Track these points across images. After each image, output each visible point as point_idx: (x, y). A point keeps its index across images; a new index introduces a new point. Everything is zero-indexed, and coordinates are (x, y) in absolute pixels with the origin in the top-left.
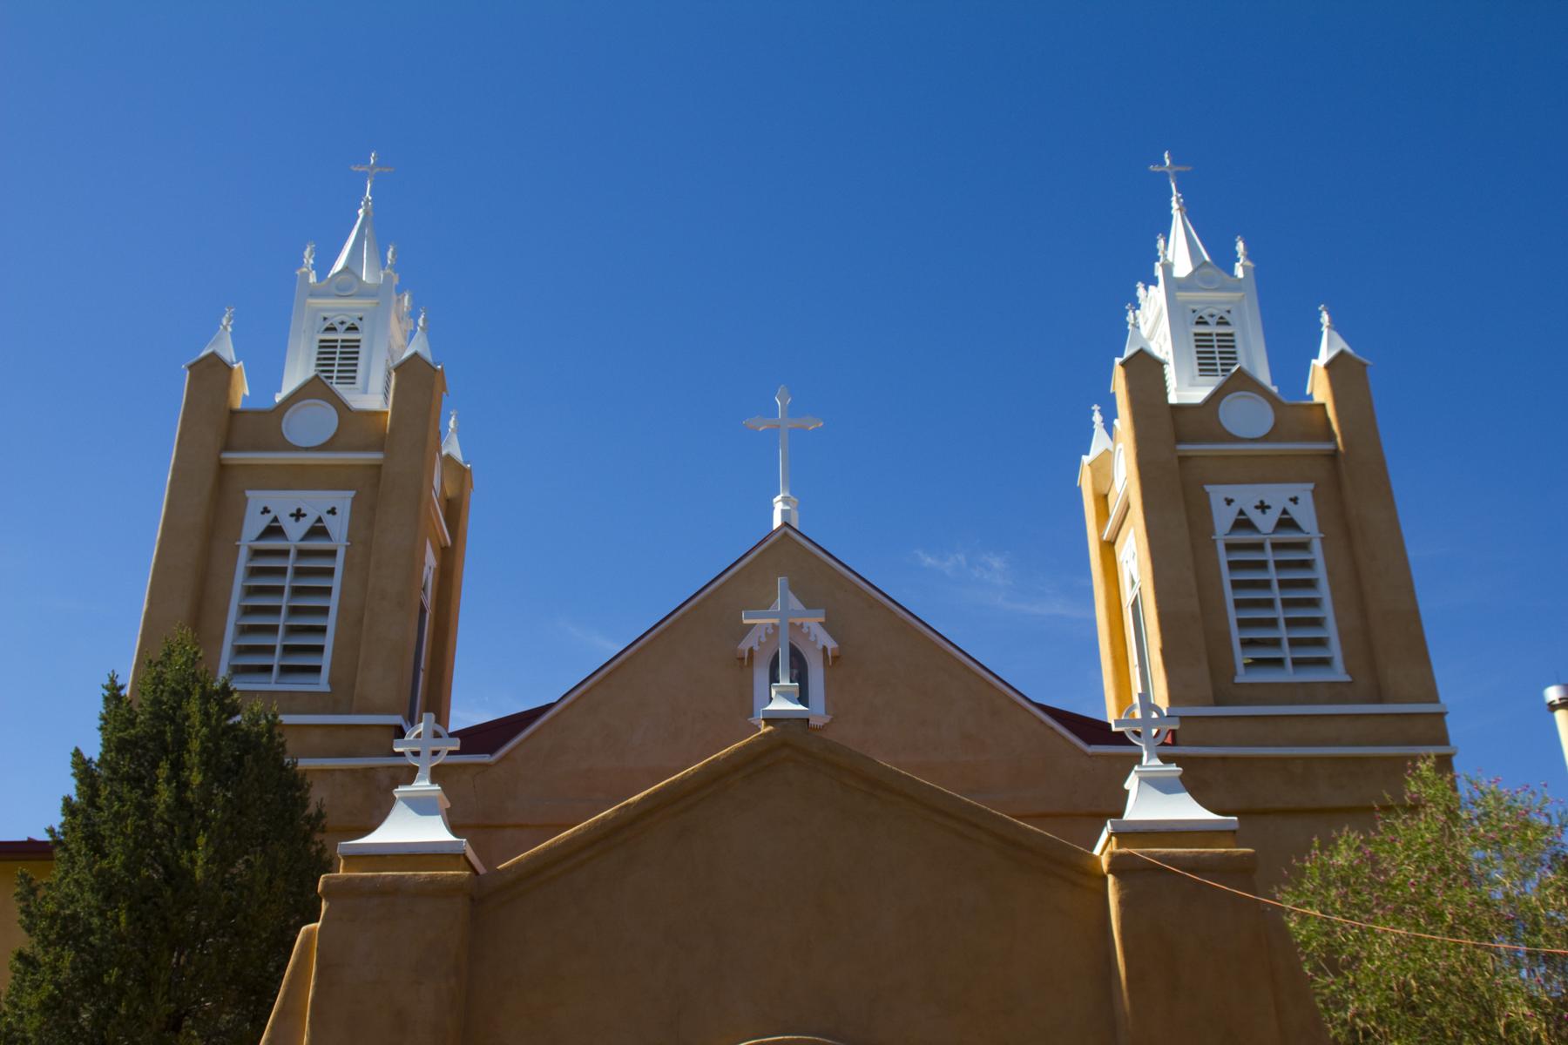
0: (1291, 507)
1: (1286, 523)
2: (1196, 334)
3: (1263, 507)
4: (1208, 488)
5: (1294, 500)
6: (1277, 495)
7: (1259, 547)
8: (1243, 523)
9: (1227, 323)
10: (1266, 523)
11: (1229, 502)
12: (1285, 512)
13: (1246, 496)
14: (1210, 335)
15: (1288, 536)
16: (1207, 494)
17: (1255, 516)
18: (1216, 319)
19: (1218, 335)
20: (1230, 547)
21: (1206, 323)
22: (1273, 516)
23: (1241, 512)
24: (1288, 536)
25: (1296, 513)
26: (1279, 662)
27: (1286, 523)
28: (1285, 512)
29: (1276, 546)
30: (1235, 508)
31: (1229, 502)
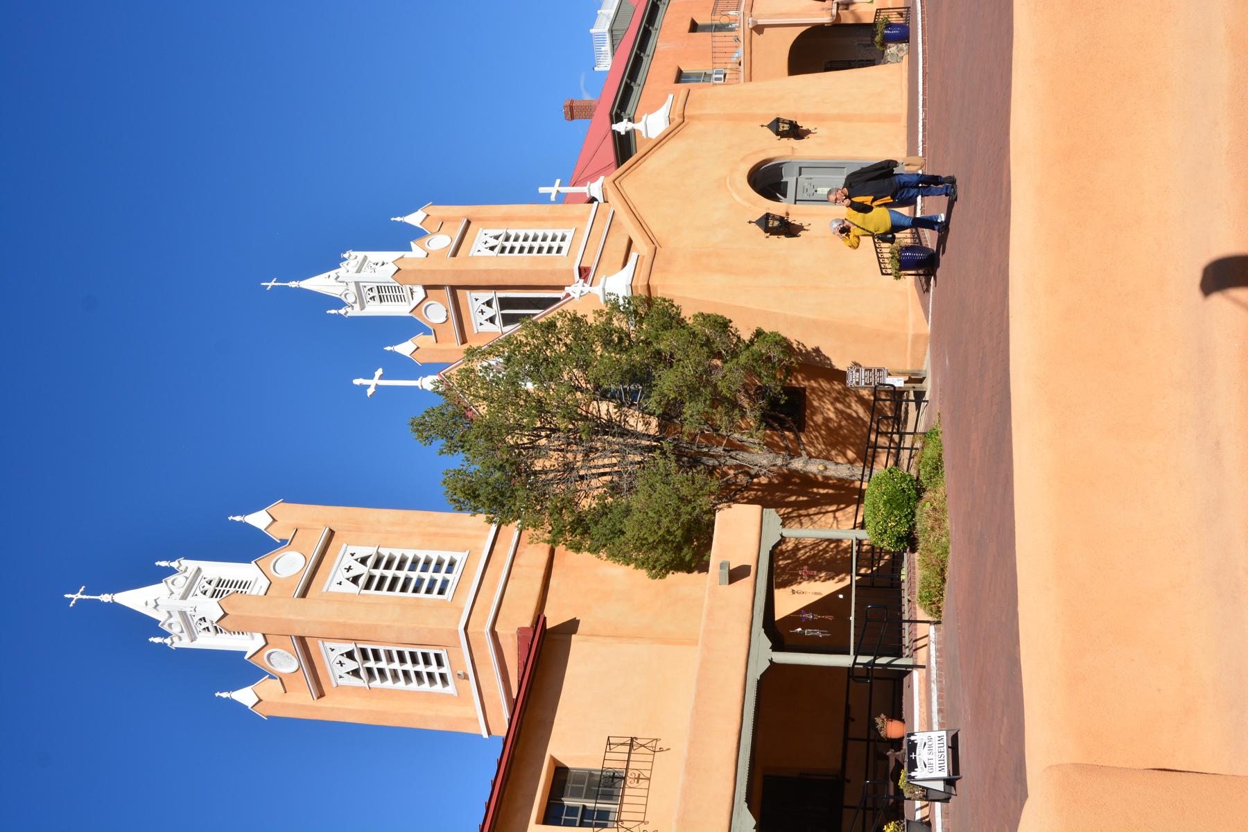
0: (355, 557)
1: (363, 561)
2: (212, 597)
3: (349, 569)
7: (371, 578)
8: (355, 580)
9: (211, 581)
10: (358, 569)
11: (340, 584)
12: (357, 560)
14: (216, 590)
15: (370, 562)
19: (218, 586)
20: (367, 587)
21: (206, 591)
23: (348, 579)
24: (370, 562)
25: (359, 555)
26: (445, 582)
27: (363, 561)
28: (357, 560)
30: (346, 583)
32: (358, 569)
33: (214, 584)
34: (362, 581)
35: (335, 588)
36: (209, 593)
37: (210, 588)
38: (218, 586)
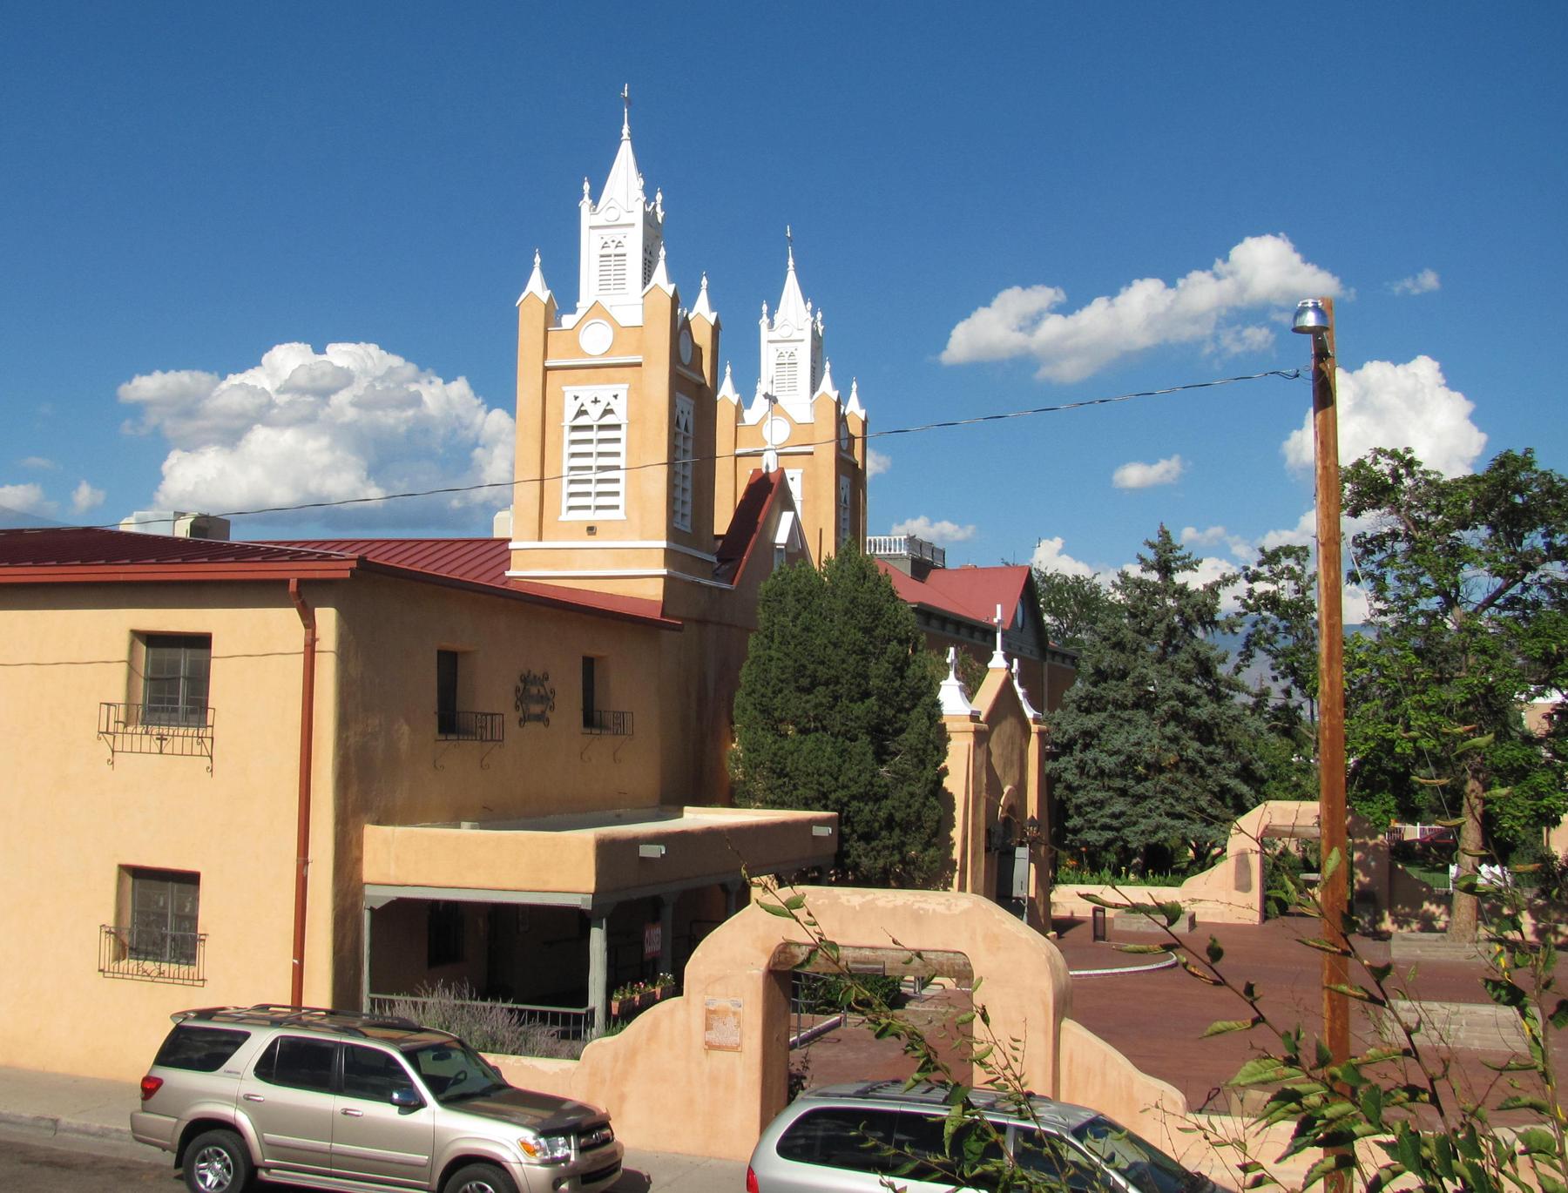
2: (602, 256)
4: (564, 388)
5: (616, 397)
6: (605, 393)
7: (590, 428)
11: (576, 398)
12: (609, 404)
13: (586, 393)
14: (610, 256)
16: (564, 392)
17: (589, 407)
18: (615, 244)
19: (616, 255)
20: (575, 428)
22: (600, 408)
23: (582, 405)
24: (608, 420)
27: (607, 412)
29: (601, 427)
30: (579, 402)
31: (576, 398)
32: (595, 412)
33: (619, 251)
34: (582, 421)
35: (569, 398)
36: (606, 251)
37: (611, 250)
38: (616, 255)
